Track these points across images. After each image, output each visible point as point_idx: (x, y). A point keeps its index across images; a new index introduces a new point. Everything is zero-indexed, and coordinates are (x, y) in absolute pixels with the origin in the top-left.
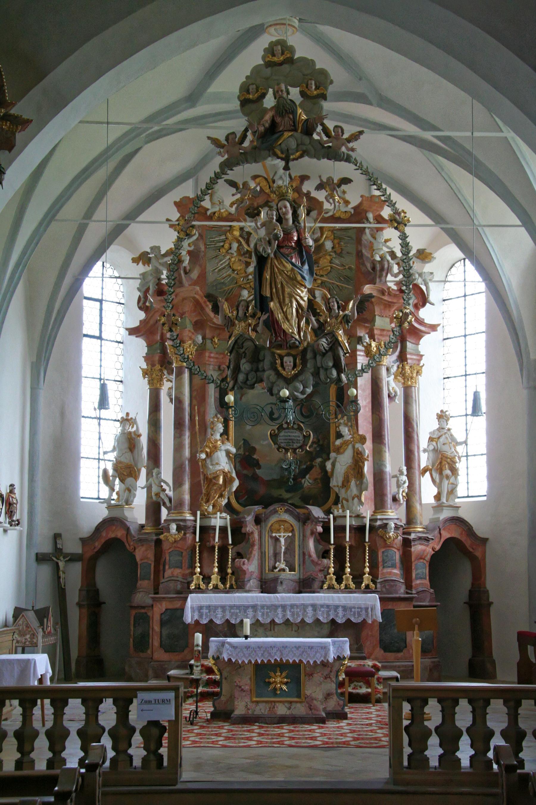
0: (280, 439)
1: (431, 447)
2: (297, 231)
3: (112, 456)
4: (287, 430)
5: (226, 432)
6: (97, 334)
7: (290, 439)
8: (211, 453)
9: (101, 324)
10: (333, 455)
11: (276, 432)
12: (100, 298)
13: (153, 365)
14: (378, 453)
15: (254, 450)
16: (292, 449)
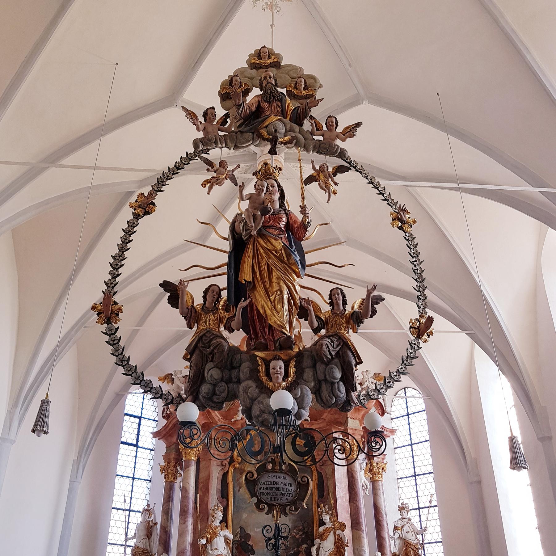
0: (261, 488)
1: (397, 535)
2: (286, 214)
3: (132, 543)
4: (272, 474)
5: (225, 520)
6: (134, 442)
7: (277, 489)
8: (211, 538)
9: (138, 435)
10: (317, 541)
11: (255, 476)
12: (140, 415)
13: (169, 462)
14: (357, 539)
15: (248, 536)
16: (280, 505)
